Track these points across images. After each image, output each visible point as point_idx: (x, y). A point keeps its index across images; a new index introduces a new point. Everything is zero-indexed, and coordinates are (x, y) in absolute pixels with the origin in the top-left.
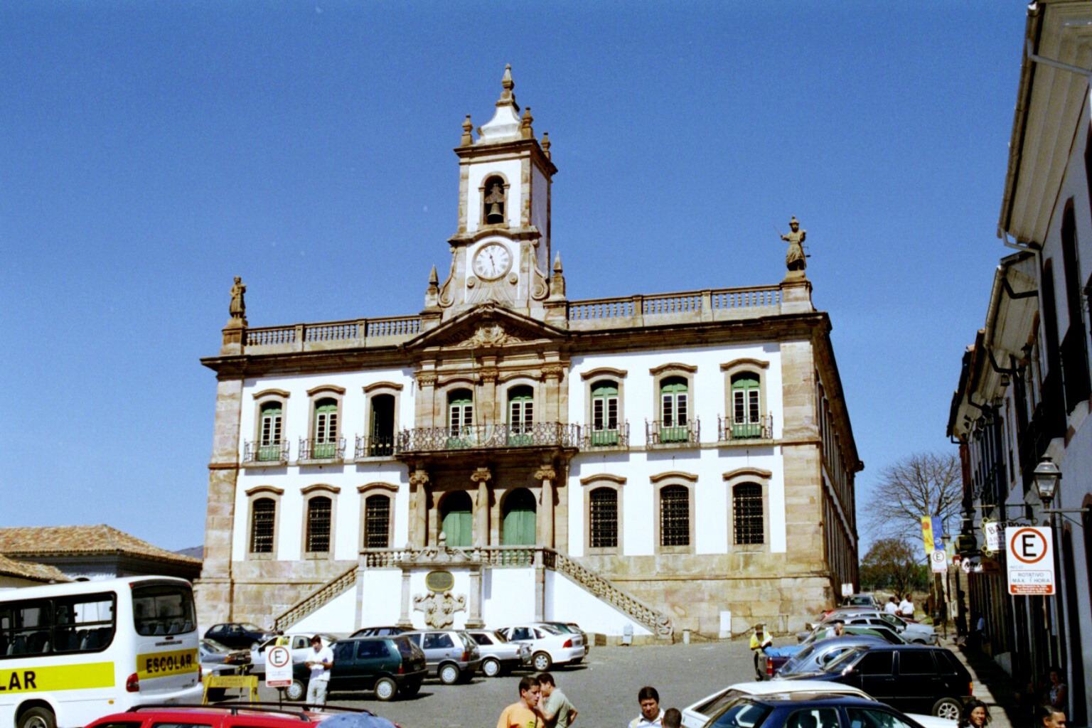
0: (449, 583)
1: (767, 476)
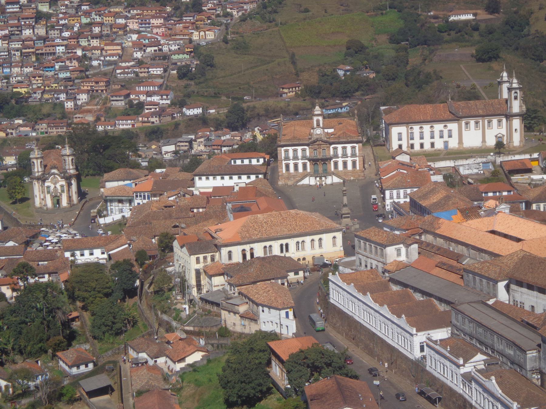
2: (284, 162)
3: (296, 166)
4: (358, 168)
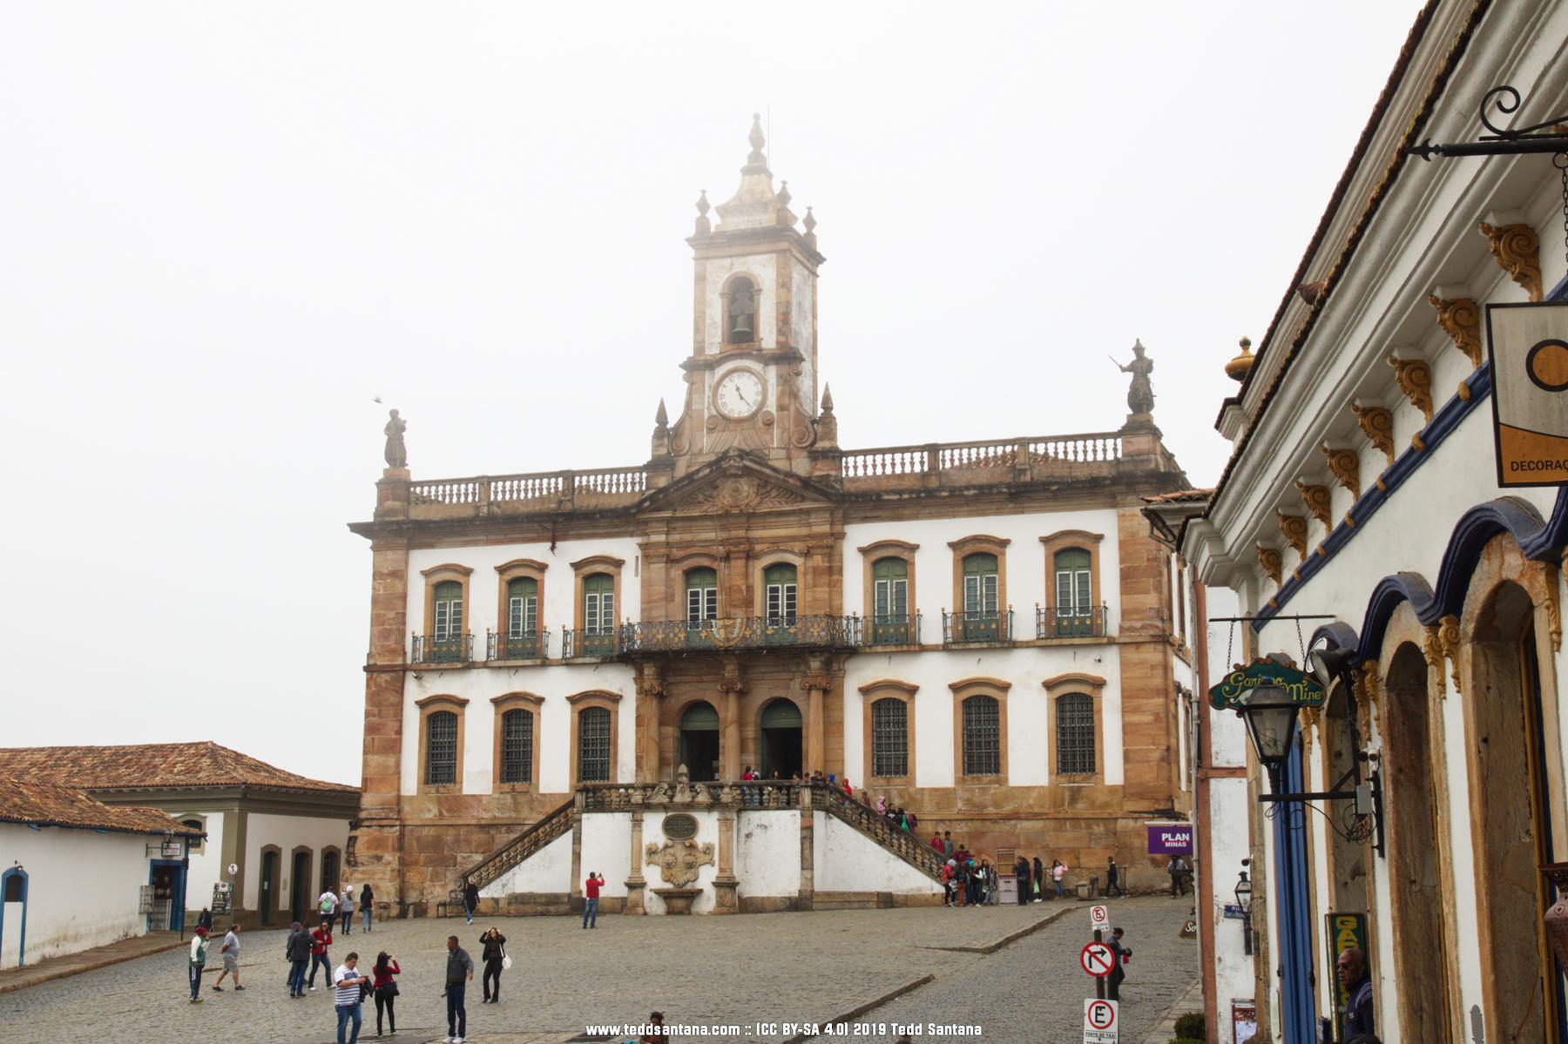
0: (691, 827)
1: (1099, 684)
2: (414, 691)
3: (517, 721)
4: (1113, 769)
